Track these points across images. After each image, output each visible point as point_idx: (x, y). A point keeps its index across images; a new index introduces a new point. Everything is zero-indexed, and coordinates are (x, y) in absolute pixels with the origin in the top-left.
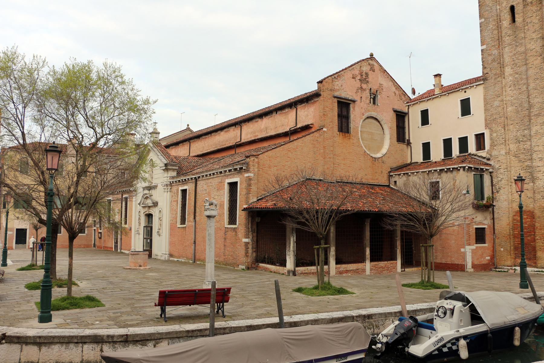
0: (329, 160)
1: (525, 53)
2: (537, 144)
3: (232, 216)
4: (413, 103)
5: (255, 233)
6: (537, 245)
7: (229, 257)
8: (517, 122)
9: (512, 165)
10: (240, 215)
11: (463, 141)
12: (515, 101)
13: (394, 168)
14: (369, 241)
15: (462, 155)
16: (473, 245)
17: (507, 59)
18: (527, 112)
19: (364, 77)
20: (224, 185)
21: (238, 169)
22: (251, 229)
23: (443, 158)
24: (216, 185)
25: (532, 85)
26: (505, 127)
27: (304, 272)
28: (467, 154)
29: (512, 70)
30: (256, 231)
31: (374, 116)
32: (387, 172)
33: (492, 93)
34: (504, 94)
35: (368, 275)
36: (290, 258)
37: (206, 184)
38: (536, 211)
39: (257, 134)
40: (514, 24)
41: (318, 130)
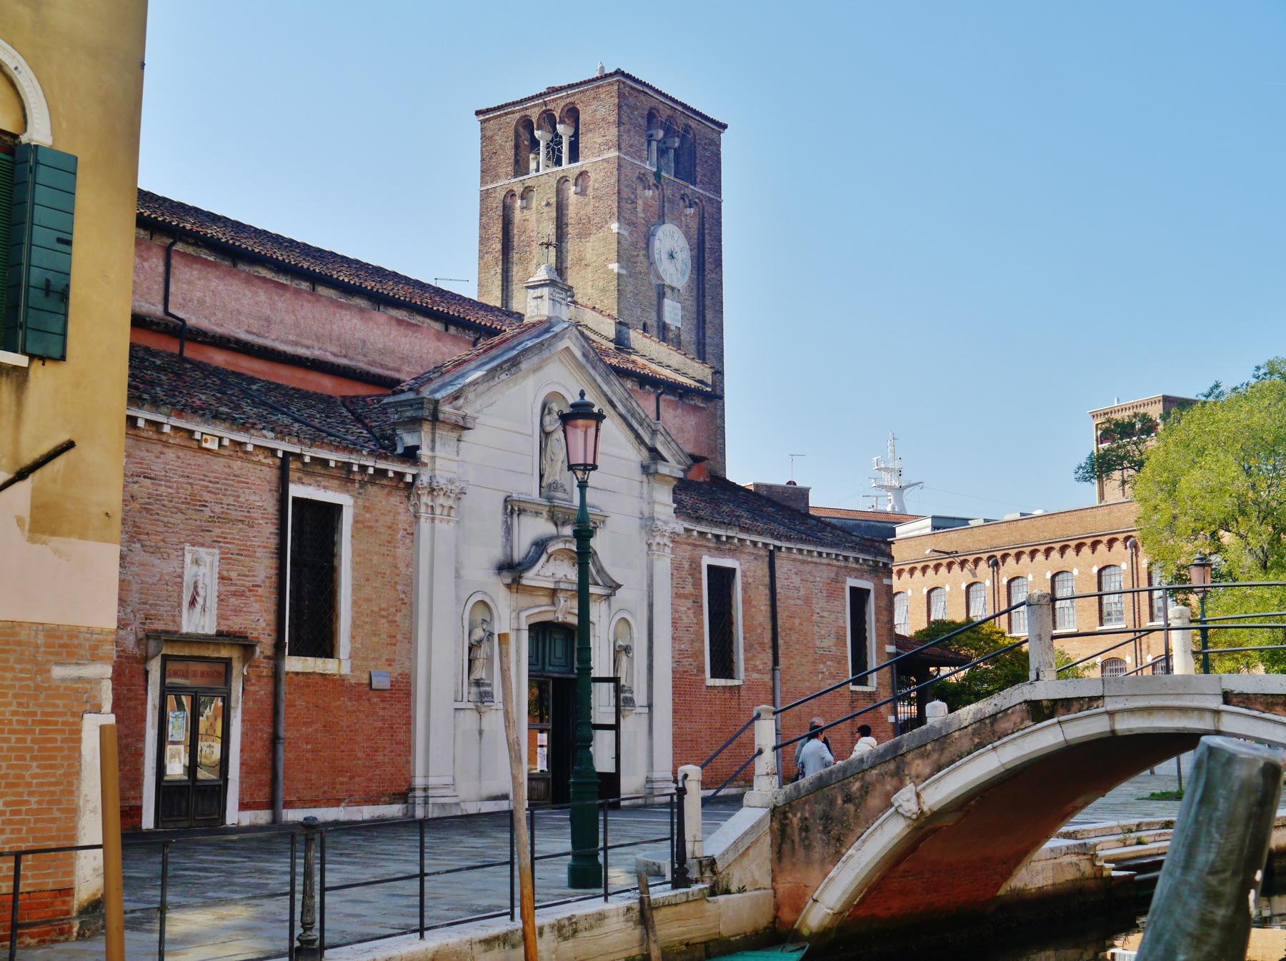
37: (796, 574)
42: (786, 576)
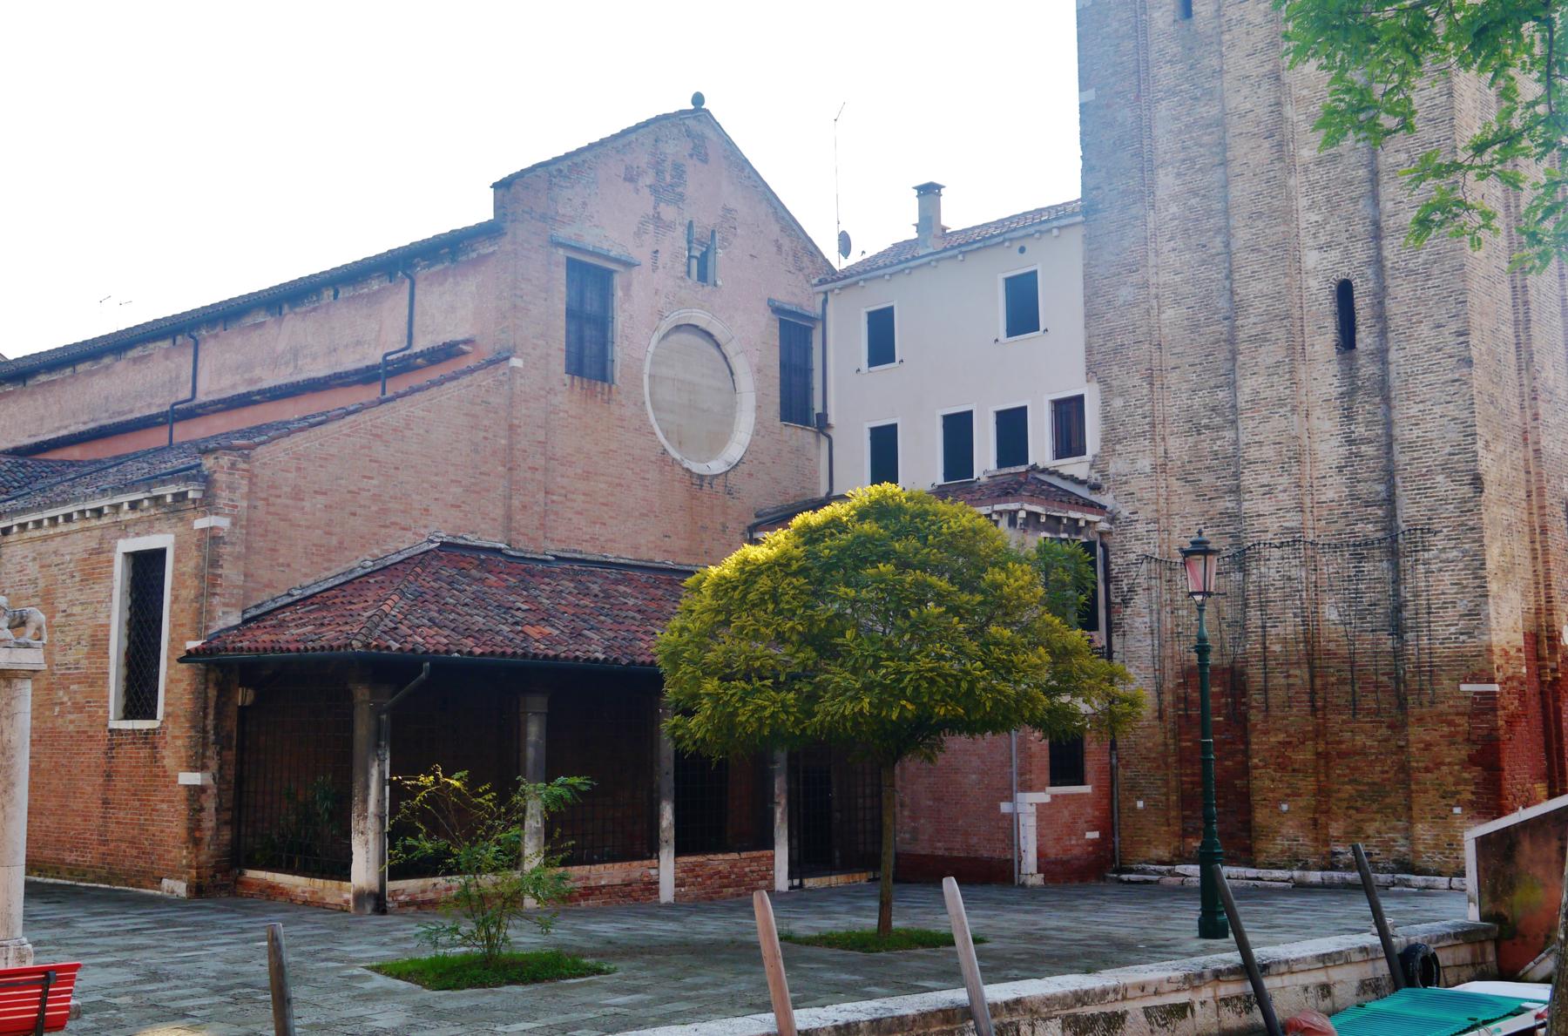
0: (529, 475)
1: (1220, 123)
2: (1257, 439)
3: (140, 686)
4: (840, 284)
5: (230, 749)
6: (1256, 784)
7: (124, 846)
8: (1191, 360)
9: (1175, 508)
10: (171, 681)
11: (1012, 425)
12: (1187, 289)
13: (769, 514)
14: (672, 776)
15: (1006, 470)
16: (1042, 789)
17: (1164, 141)
18: (1223, 328)
19: (668, 179)
20: (110, 562)
21: (169, 499)
22: (217, 734)
23: (940, 480)
24: (78, 561)
25: (1242, 236)
26: (1151, 376)
27: (420, 897)
28: (1022, 469)
29: (1178, 182)
30: (234, 743)
31: (703, 325)
32: (742, 527)
33: (1113, 258)
34: (1152, 260)
35: (668, 906)
36: (367, 843)
37: (34, 559)
38: (1251, 671)
39: (258, 372)
40: (1187, 22)
41: (491, 362)
42: (19, 568)
